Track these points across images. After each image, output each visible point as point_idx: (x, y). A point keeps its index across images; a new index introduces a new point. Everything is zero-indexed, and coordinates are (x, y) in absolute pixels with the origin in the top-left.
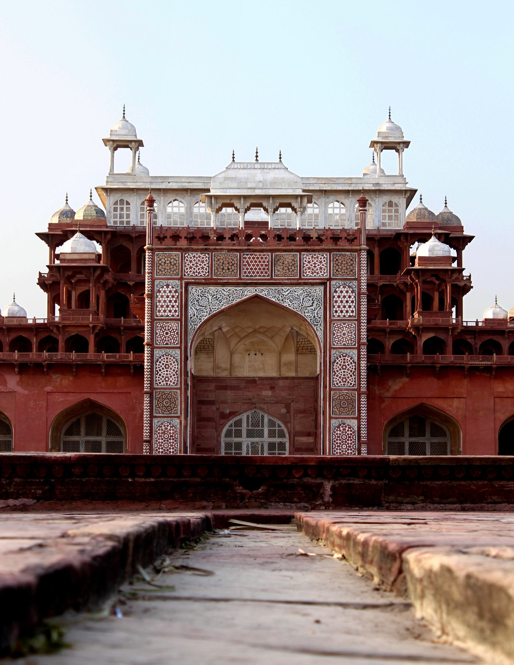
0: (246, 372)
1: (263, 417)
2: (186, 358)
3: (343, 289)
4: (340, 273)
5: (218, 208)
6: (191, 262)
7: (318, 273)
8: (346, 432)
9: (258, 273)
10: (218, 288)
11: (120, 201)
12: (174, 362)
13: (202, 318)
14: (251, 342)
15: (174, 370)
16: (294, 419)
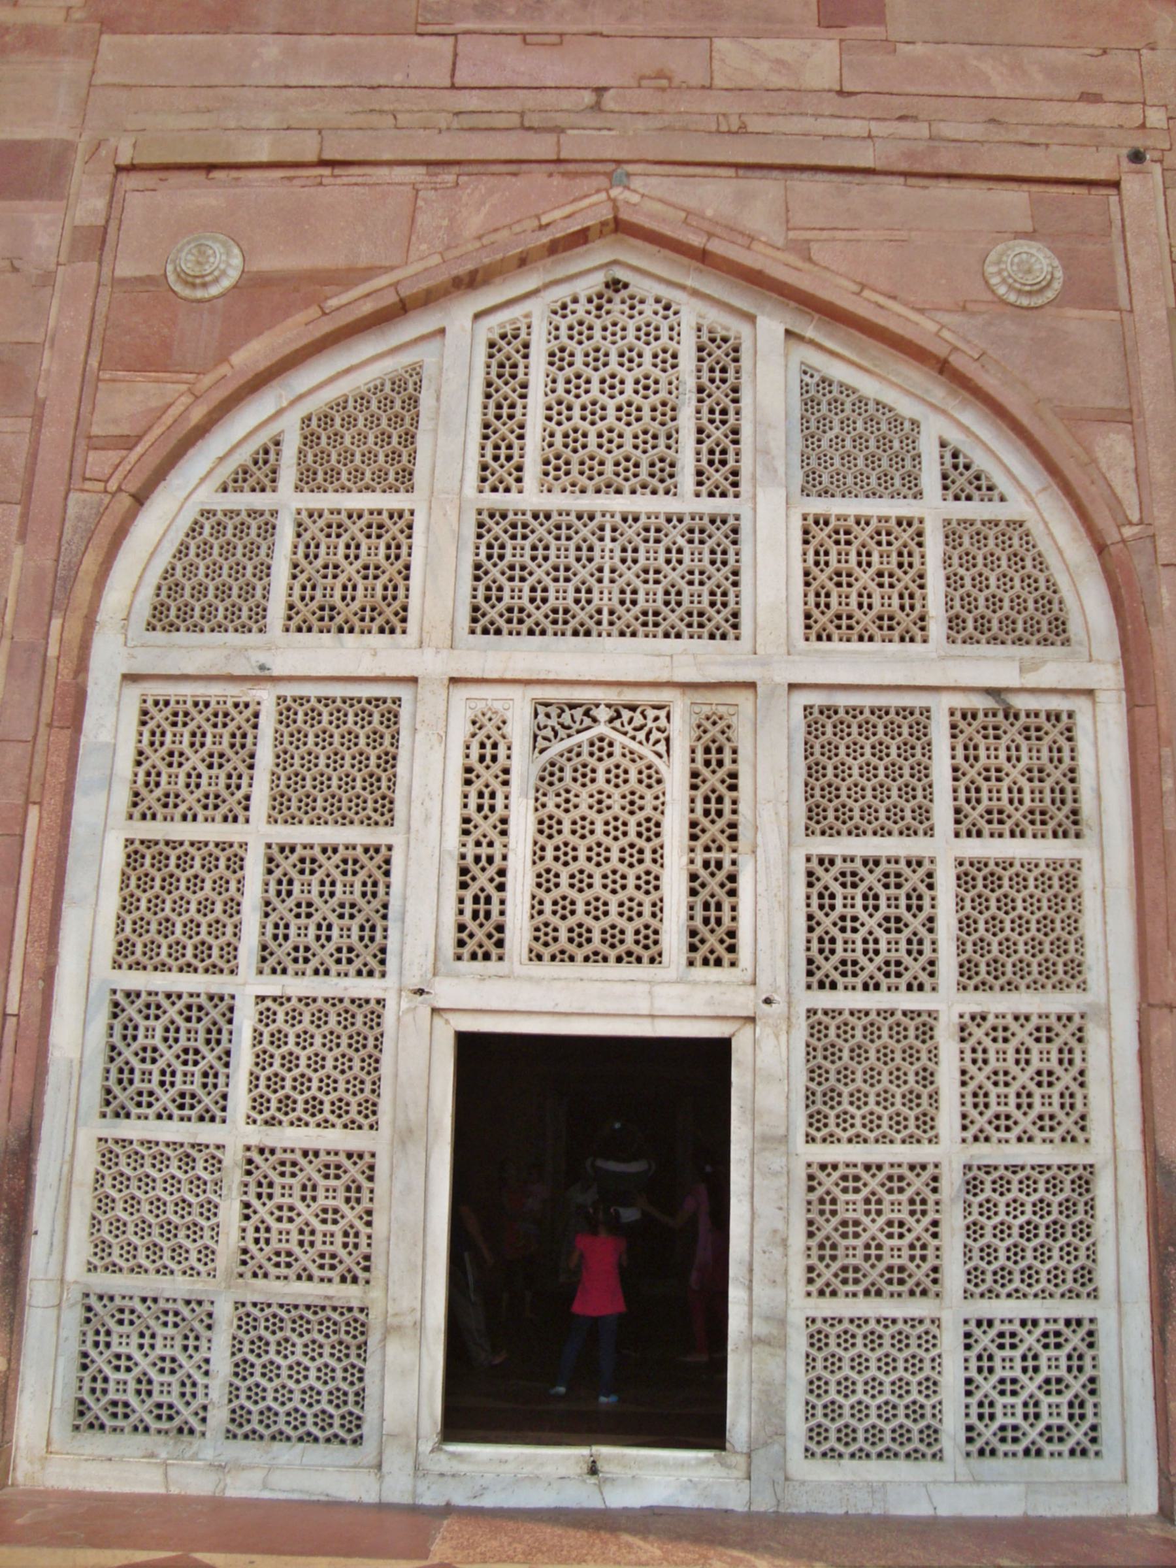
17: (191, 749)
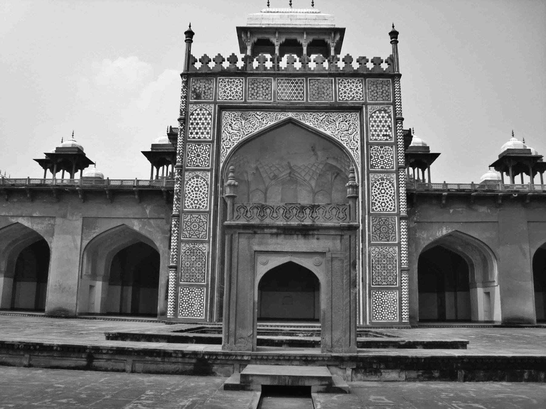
13: (235, 142)
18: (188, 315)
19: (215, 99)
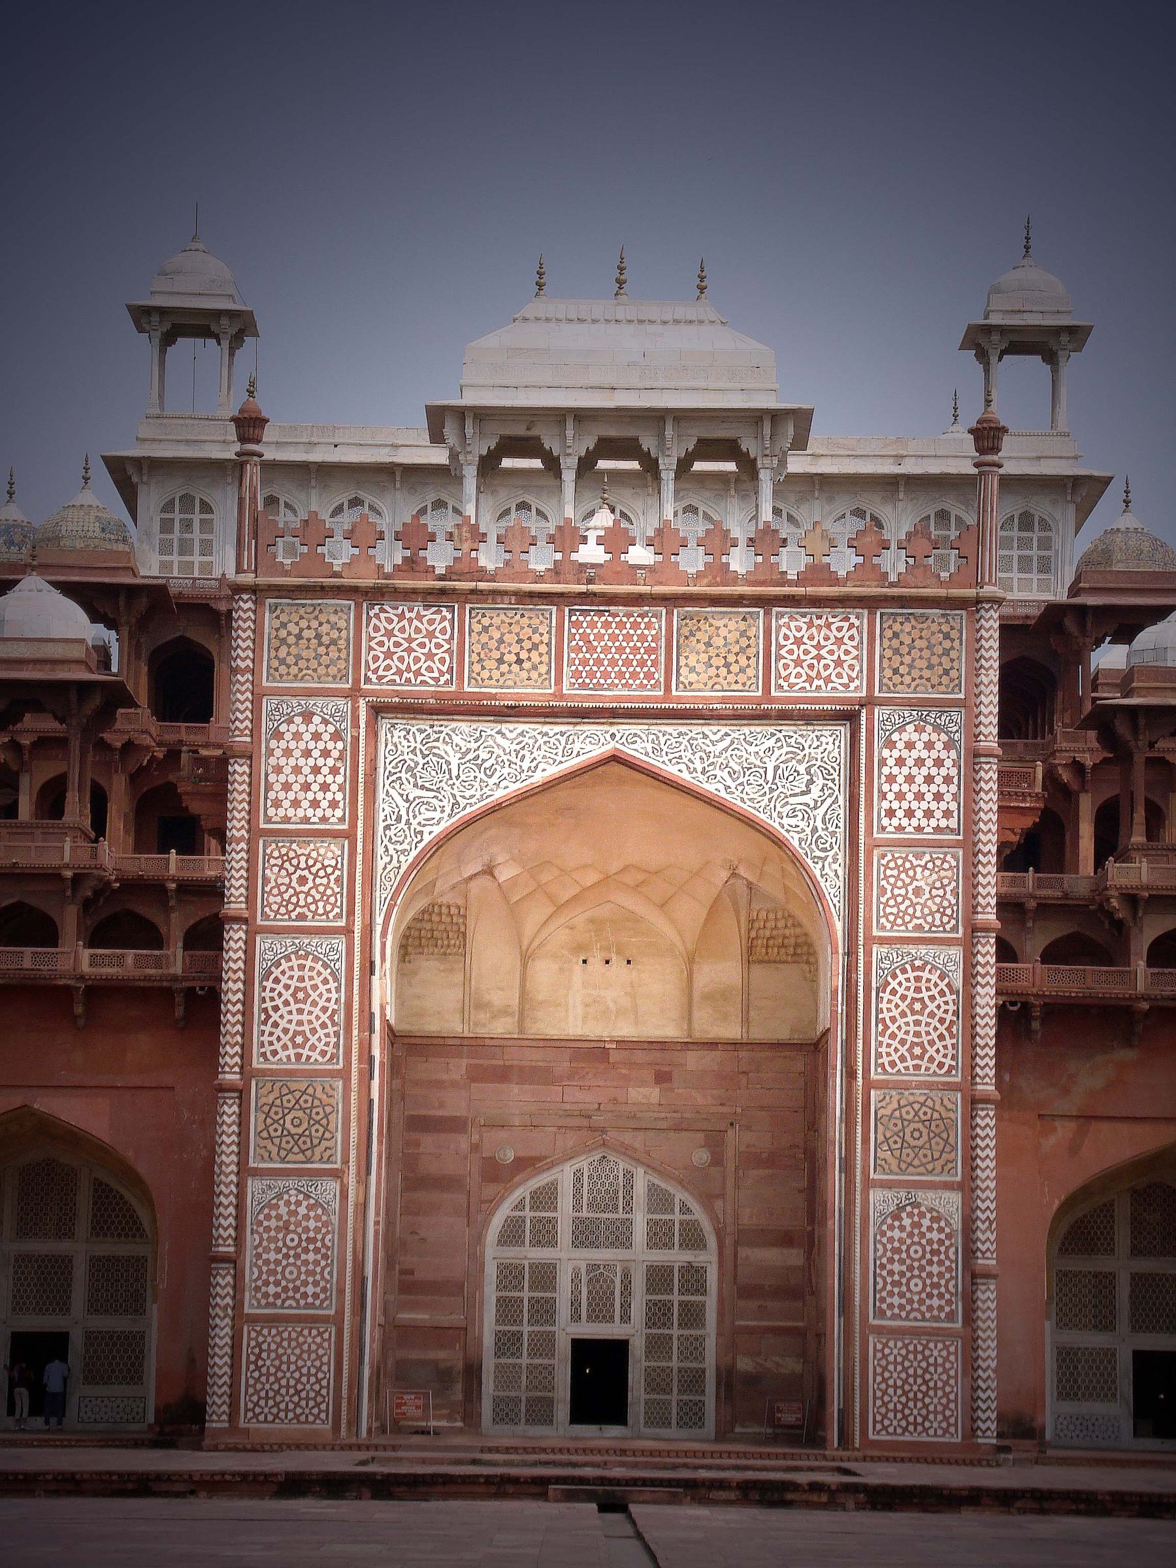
0: (574, 1023)
1: (629, 1177)
2: (369, 968)
3: (915, 737)
4: (907, 680)
5: (485, 452)
6: (389, 634)
7: (828, 680)
8: (922, 1235)
9: (621, 675)
10: (481, 726)
11: (181, 498)
12: (325, 981)
13: (426, 830)
14: (592, 921)
15: (324, 1010)
16: (737, 1187)
17: (510, 1275)
18: (276, 1416)
19: (357, 681)
